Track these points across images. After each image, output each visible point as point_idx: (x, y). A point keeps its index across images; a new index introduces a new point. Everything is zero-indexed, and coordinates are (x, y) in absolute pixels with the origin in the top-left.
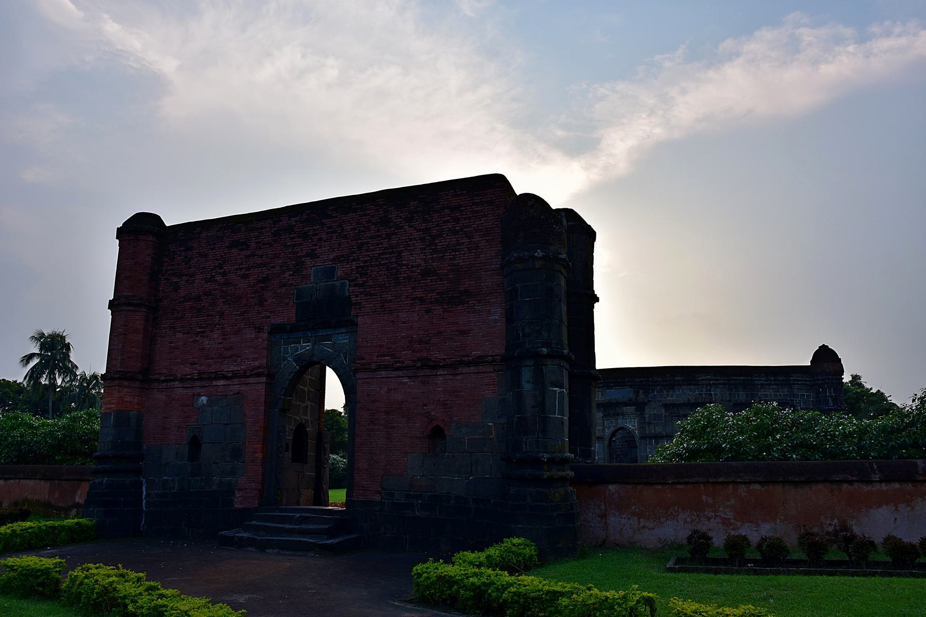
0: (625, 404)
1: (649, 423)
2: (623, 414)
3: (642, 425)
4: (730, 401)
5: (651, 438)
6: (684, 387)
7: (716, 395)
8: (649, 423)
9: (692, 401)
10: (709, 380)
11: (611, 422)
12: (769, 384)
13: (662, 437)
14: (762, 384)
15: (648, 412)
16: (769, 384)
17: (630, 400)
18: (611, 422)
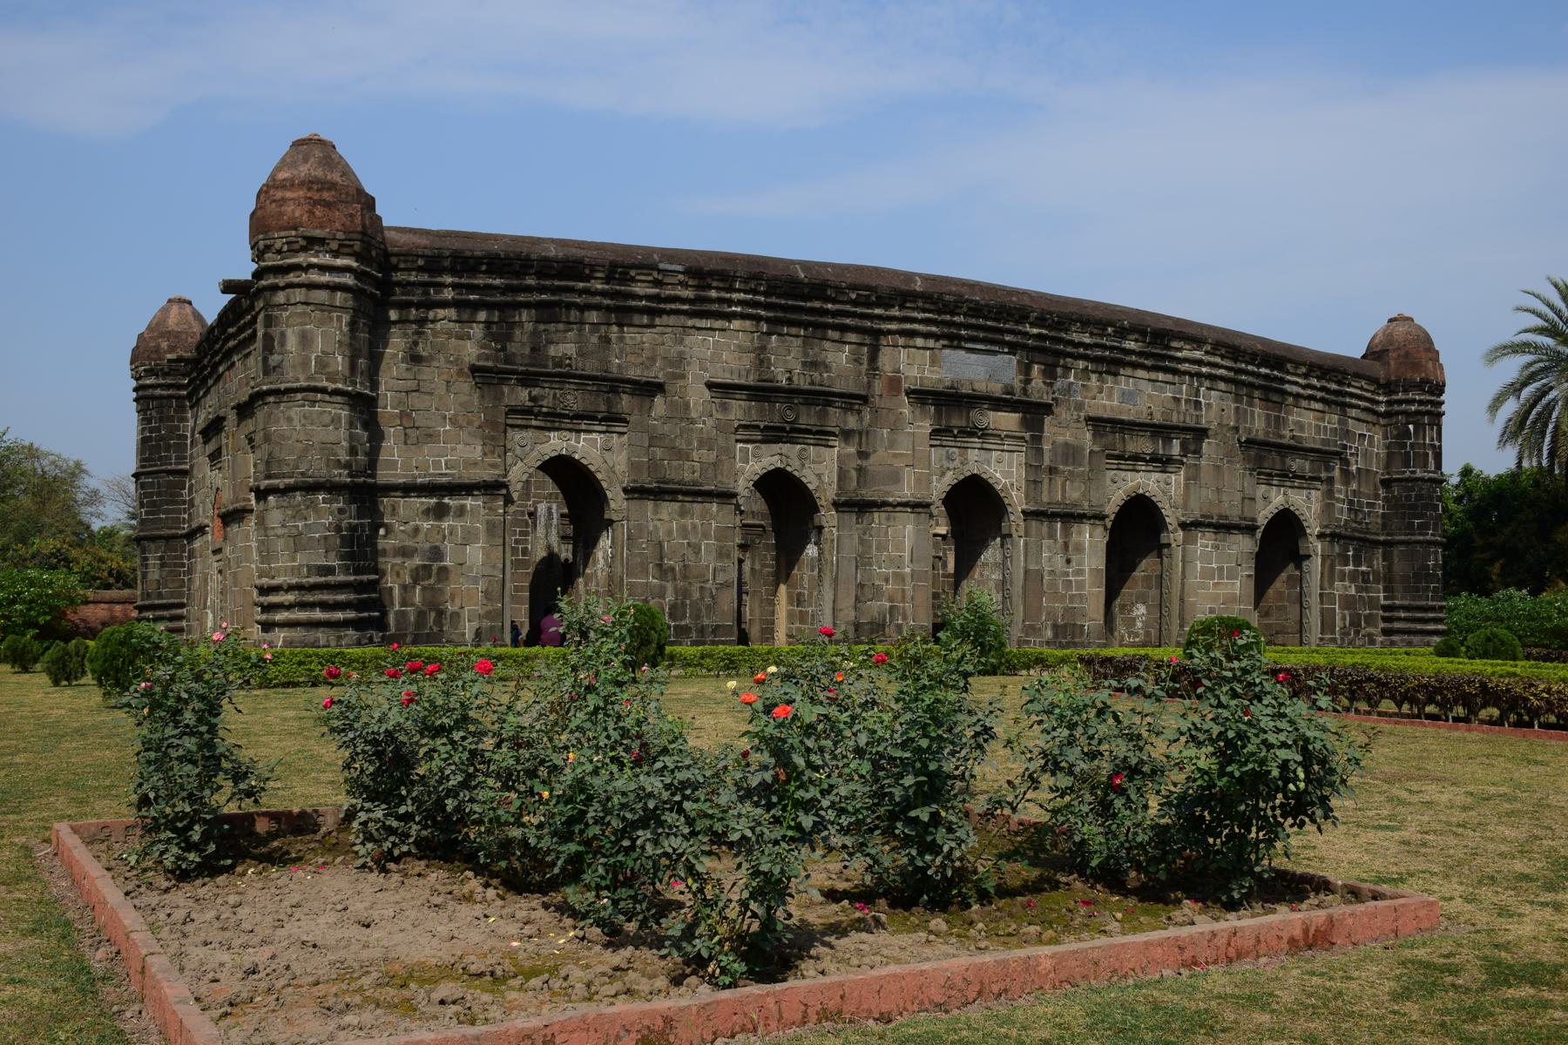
0: (998, 404)
1: (1052, 471)
2: (984, 434)
3: (1037, 472)
4: (1236, 429)
5: (1052, 517)
6: (1141, 373)
7: (1209, 405)
8: (1052, 471)
9: (1158, 419)
10: (1200, 362)
11: (950, 458)
12: (1311, 398)
13: (1081, 518)
14: (1297, 396)
15: (1057, 432)
16: (1311, 398)
17: (1009, 390)
18: (950, 458)
